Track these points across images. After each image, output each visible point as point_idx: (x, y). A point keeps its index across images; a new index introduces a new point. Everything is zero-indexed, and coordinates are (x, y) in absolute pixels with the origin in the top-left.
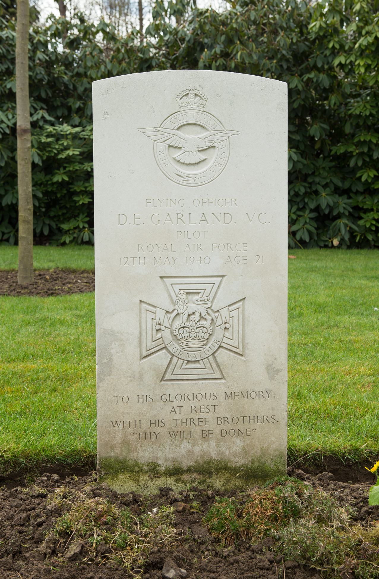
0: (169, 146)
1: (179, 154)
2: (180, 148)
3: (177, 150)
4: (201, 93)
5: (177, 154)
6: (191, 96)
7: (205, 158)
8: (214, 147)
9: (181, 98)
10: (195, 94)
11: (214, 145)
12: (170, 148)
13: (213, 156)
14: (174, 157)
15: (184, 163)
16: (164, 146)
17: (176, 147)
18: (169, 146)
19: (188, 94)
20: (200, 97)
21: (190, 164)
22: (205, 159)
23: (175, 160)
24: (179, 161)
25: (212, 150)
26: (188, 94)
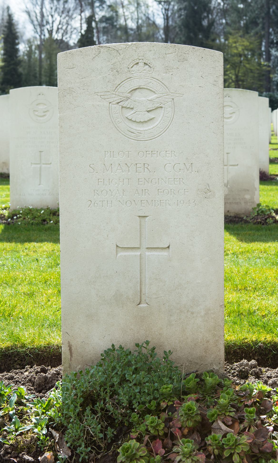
0: (122, 107)
1: (130, 114)
2: (132, 109)
3: (129, 110)
4: (149, 62)
5: (129, 114)
6: (141, 64)
7: (153, 117)
8: (161, 107)
9: (132, 67)
10: (145, 63)
11: (160, 106)
12: (124, 110)
13: (159, 115)
14: (127, 116)
15: (135, 121)
16: (118, 107)
17: (128, 108)
18: (122, 107)
19: (138, 63)
20: (148, 65)
21: (140, 122)
22: (153, 118)
23: (128, 118)
24: (131, 120)
25: (158, 110)
26: (138, 63)
